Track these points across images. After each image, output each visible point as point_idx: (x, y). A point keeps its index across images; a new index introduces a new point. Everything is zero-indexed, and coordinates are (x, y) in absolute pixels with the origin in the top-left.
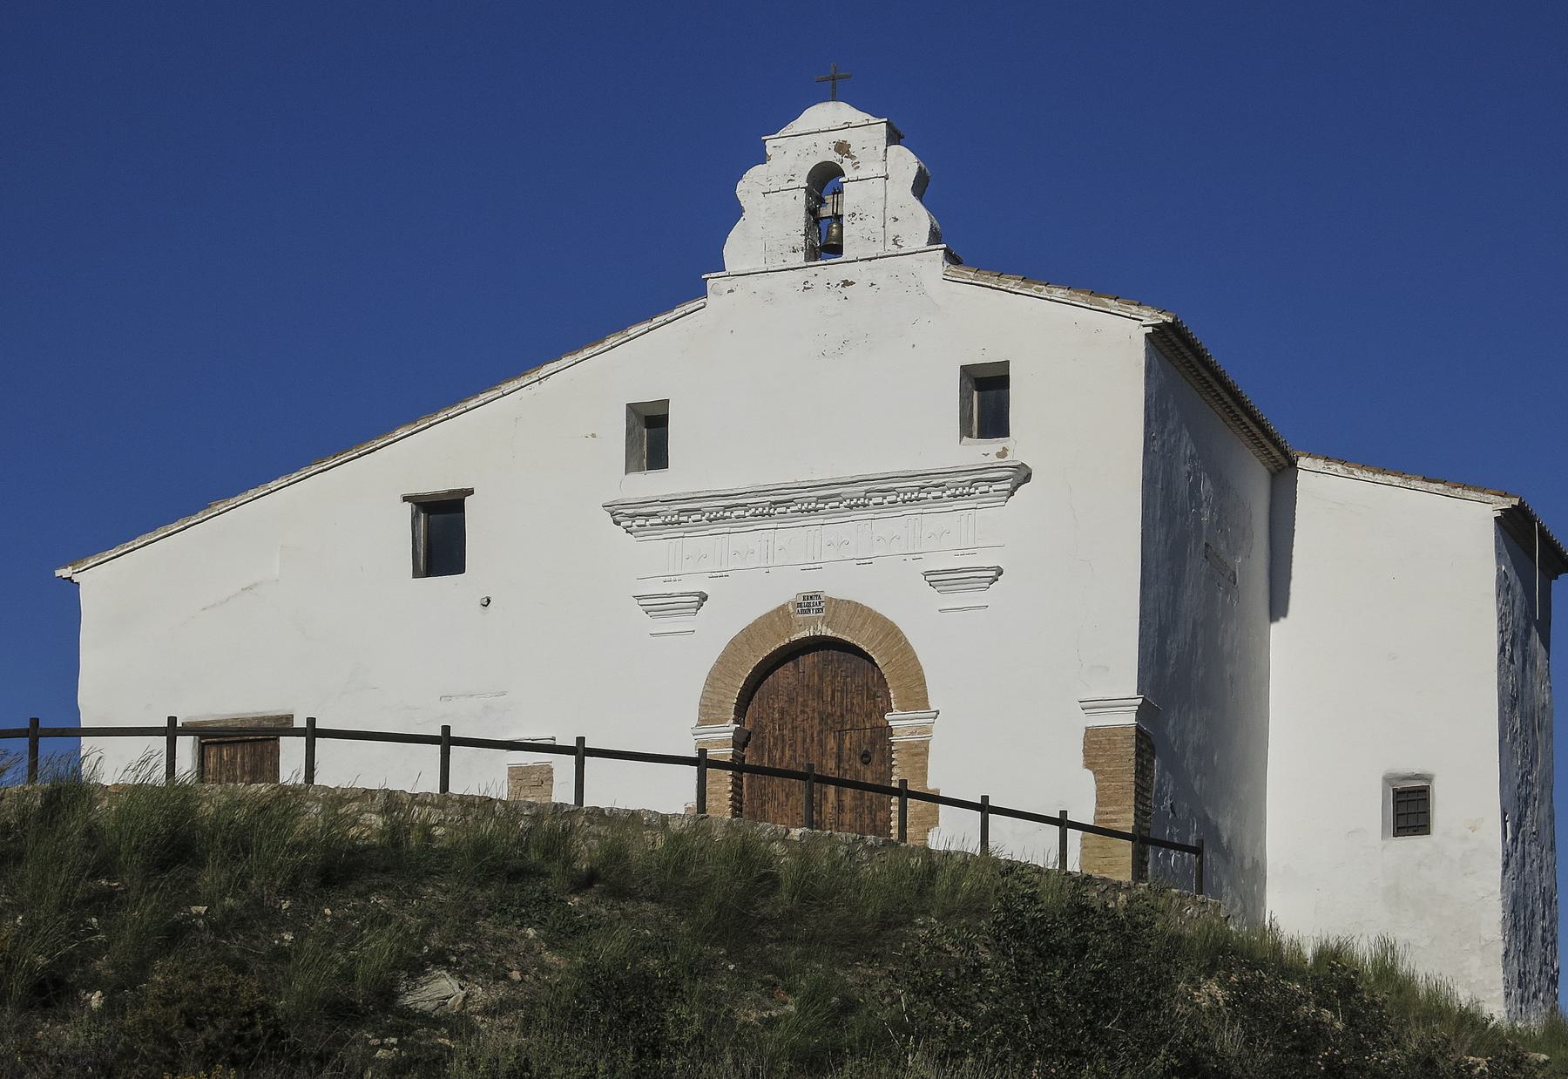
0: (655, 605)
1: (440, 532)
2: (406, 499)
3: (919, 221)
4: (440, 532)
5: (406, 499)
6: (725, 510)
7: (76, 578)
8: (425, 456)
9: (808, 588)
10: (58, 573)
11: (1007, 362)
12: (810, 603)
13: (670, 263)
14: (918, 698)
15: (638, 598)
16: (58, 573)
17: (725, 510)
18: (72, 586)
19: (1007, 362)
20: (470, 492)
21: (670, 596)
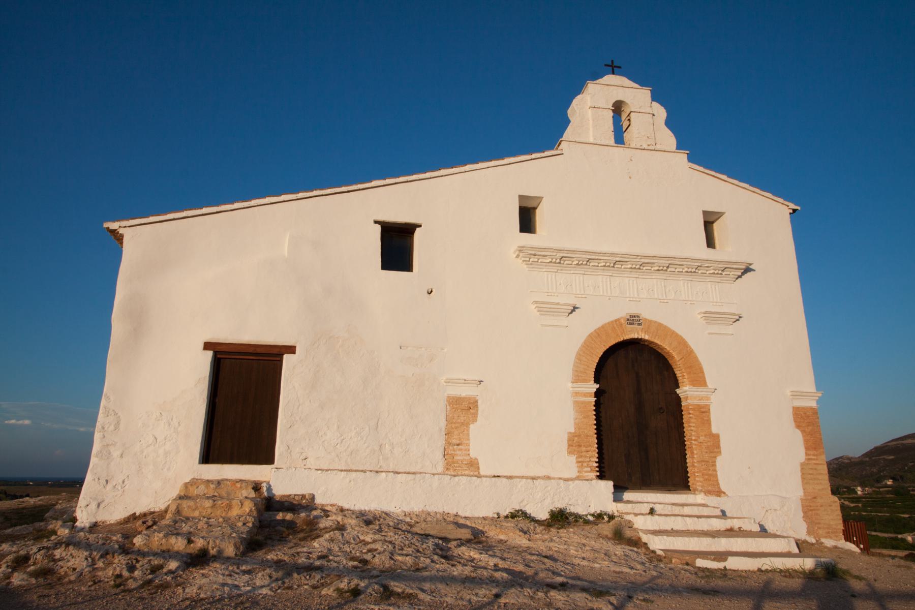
0: (545, 309)
1: (397, 247)
2: (376, 222)
3: (669, 139)
4: (397, 247)
5: (376, 222)
6: (562, 259)
7: (121, 231)
8: (394, 200)
9: (634, 311)
10: (106, 225)
11: (520, 196)
12: (633, 320)
13: (542, 131)
14: (699, 380)
15: (536, 302)
16: (106, 225)
17: (562, 259)
18: (118, 238)
19: (520, 196)
20: (420, 226)
21: (558, 304)
